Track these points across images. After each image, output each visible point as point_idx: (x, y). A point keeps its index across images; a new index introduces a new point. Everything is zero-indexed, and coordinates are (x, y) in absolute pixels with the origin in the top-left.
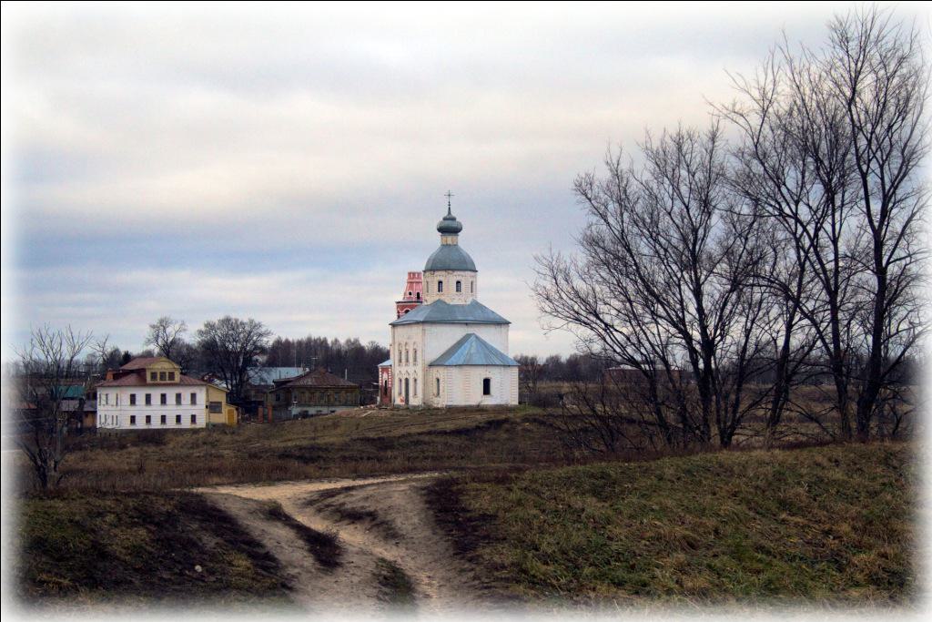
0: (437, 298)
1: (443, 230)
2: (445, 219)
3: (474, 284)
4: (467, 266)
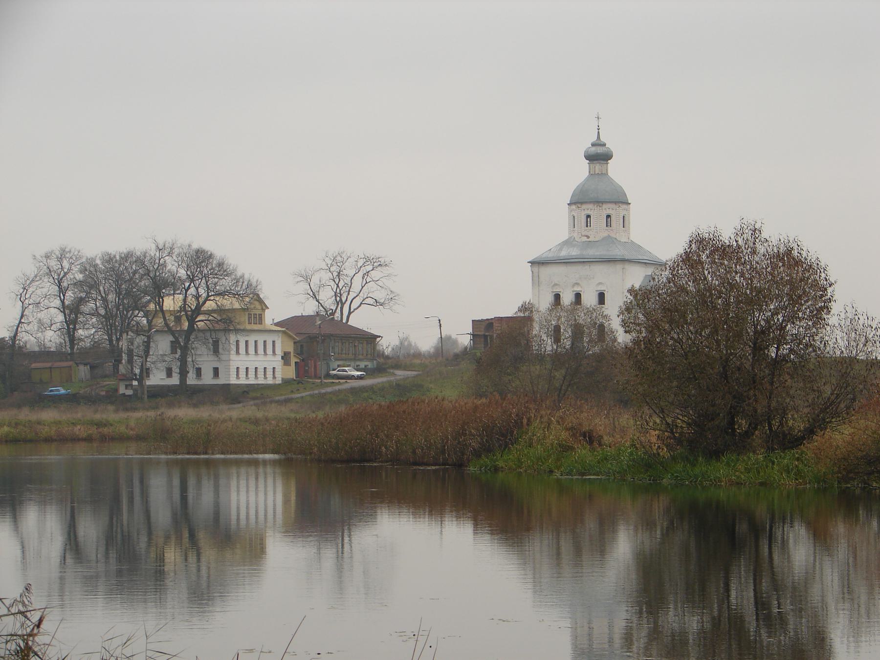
0: (605, 234)
1: (591, 158)
2: (593, 145)
3: (626, 218)
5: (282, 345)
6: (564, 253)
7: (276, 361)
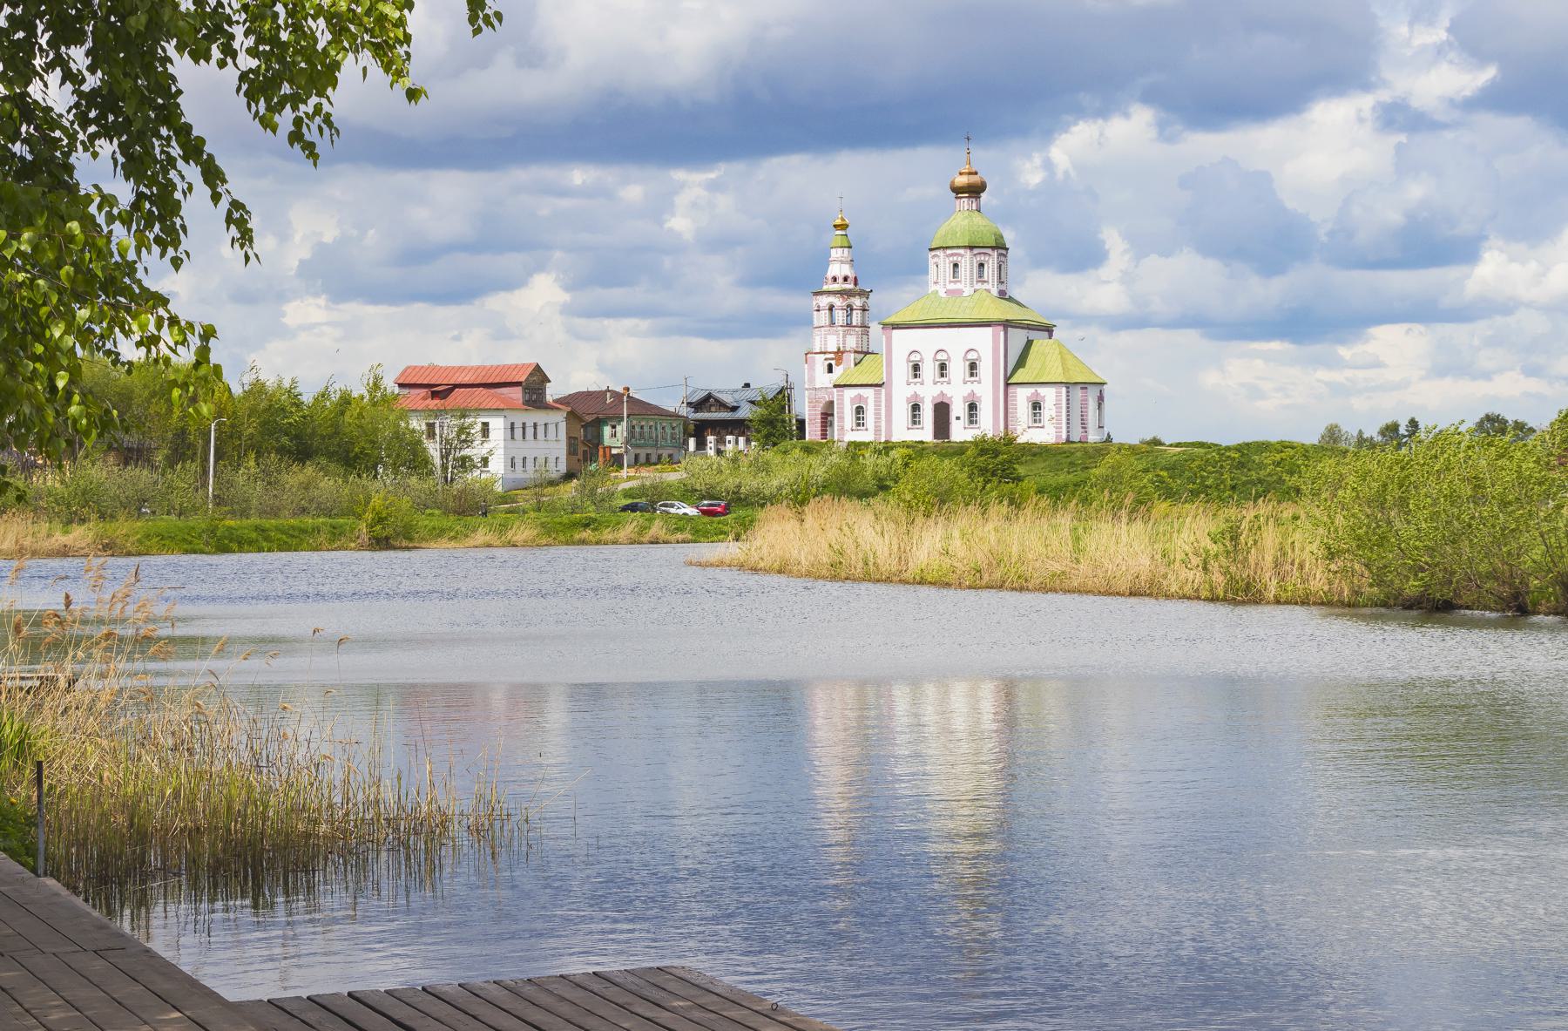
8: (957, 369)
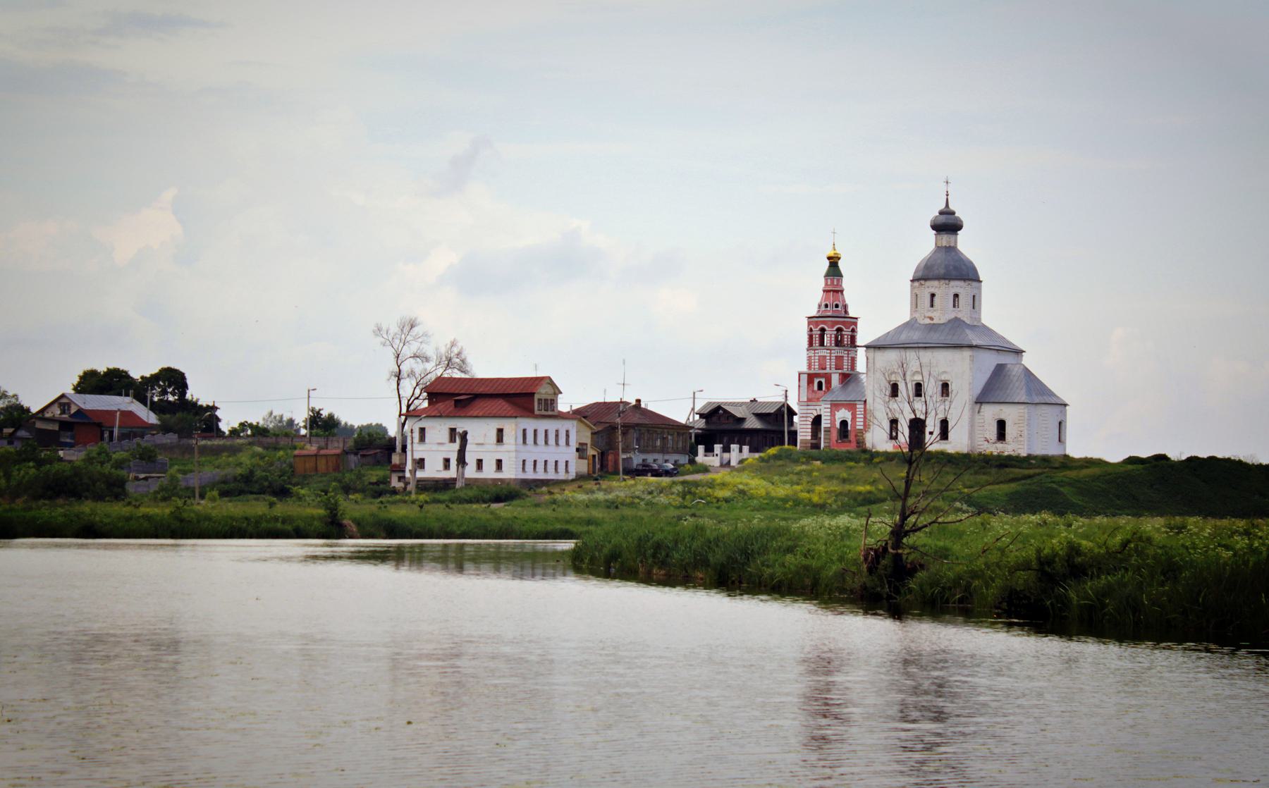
2: (941, 213)
4: (965, 273)
5: (579, 433)
6: (904, 338)
7: (570, 454)
8: (932, 389)
